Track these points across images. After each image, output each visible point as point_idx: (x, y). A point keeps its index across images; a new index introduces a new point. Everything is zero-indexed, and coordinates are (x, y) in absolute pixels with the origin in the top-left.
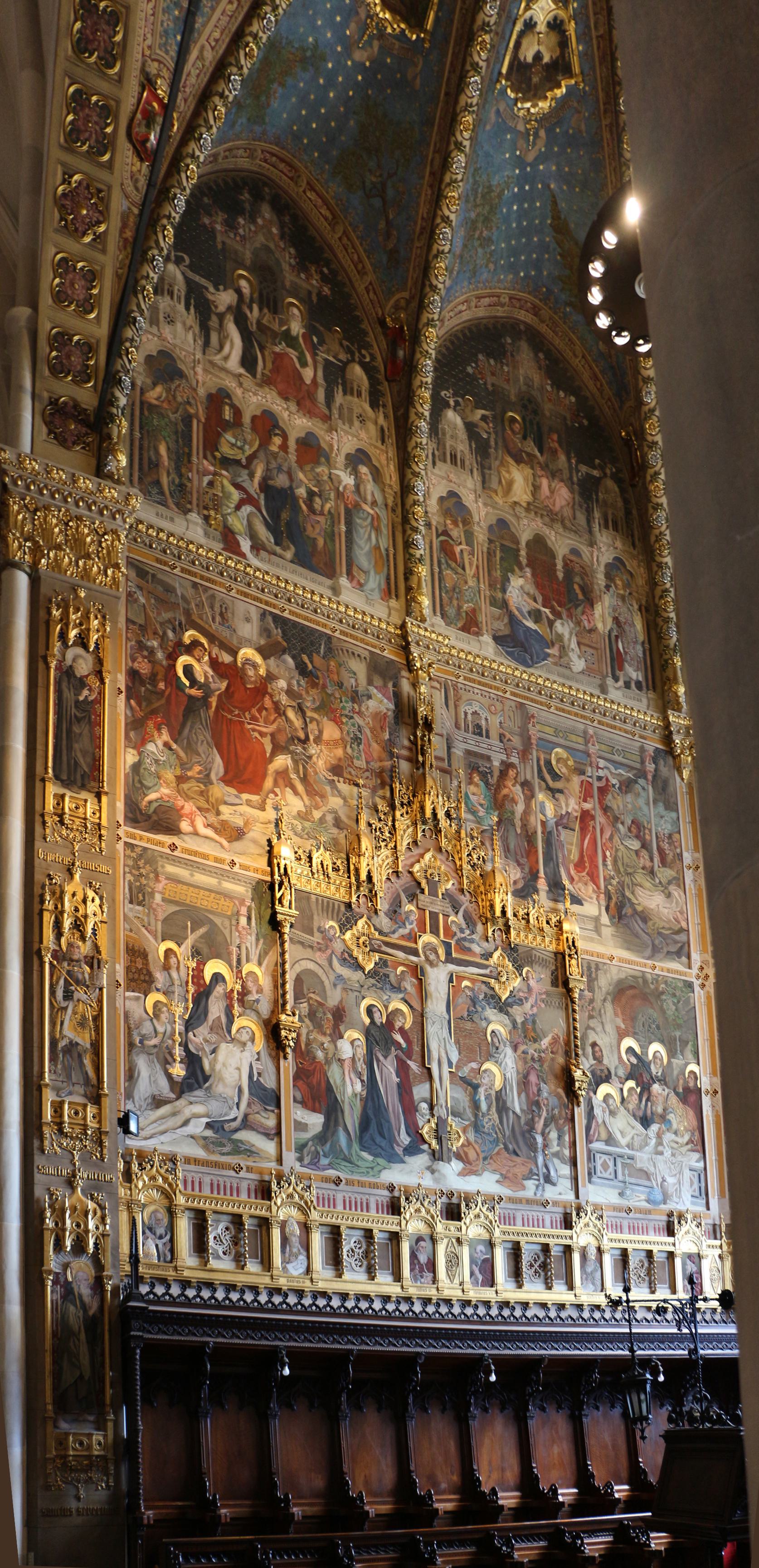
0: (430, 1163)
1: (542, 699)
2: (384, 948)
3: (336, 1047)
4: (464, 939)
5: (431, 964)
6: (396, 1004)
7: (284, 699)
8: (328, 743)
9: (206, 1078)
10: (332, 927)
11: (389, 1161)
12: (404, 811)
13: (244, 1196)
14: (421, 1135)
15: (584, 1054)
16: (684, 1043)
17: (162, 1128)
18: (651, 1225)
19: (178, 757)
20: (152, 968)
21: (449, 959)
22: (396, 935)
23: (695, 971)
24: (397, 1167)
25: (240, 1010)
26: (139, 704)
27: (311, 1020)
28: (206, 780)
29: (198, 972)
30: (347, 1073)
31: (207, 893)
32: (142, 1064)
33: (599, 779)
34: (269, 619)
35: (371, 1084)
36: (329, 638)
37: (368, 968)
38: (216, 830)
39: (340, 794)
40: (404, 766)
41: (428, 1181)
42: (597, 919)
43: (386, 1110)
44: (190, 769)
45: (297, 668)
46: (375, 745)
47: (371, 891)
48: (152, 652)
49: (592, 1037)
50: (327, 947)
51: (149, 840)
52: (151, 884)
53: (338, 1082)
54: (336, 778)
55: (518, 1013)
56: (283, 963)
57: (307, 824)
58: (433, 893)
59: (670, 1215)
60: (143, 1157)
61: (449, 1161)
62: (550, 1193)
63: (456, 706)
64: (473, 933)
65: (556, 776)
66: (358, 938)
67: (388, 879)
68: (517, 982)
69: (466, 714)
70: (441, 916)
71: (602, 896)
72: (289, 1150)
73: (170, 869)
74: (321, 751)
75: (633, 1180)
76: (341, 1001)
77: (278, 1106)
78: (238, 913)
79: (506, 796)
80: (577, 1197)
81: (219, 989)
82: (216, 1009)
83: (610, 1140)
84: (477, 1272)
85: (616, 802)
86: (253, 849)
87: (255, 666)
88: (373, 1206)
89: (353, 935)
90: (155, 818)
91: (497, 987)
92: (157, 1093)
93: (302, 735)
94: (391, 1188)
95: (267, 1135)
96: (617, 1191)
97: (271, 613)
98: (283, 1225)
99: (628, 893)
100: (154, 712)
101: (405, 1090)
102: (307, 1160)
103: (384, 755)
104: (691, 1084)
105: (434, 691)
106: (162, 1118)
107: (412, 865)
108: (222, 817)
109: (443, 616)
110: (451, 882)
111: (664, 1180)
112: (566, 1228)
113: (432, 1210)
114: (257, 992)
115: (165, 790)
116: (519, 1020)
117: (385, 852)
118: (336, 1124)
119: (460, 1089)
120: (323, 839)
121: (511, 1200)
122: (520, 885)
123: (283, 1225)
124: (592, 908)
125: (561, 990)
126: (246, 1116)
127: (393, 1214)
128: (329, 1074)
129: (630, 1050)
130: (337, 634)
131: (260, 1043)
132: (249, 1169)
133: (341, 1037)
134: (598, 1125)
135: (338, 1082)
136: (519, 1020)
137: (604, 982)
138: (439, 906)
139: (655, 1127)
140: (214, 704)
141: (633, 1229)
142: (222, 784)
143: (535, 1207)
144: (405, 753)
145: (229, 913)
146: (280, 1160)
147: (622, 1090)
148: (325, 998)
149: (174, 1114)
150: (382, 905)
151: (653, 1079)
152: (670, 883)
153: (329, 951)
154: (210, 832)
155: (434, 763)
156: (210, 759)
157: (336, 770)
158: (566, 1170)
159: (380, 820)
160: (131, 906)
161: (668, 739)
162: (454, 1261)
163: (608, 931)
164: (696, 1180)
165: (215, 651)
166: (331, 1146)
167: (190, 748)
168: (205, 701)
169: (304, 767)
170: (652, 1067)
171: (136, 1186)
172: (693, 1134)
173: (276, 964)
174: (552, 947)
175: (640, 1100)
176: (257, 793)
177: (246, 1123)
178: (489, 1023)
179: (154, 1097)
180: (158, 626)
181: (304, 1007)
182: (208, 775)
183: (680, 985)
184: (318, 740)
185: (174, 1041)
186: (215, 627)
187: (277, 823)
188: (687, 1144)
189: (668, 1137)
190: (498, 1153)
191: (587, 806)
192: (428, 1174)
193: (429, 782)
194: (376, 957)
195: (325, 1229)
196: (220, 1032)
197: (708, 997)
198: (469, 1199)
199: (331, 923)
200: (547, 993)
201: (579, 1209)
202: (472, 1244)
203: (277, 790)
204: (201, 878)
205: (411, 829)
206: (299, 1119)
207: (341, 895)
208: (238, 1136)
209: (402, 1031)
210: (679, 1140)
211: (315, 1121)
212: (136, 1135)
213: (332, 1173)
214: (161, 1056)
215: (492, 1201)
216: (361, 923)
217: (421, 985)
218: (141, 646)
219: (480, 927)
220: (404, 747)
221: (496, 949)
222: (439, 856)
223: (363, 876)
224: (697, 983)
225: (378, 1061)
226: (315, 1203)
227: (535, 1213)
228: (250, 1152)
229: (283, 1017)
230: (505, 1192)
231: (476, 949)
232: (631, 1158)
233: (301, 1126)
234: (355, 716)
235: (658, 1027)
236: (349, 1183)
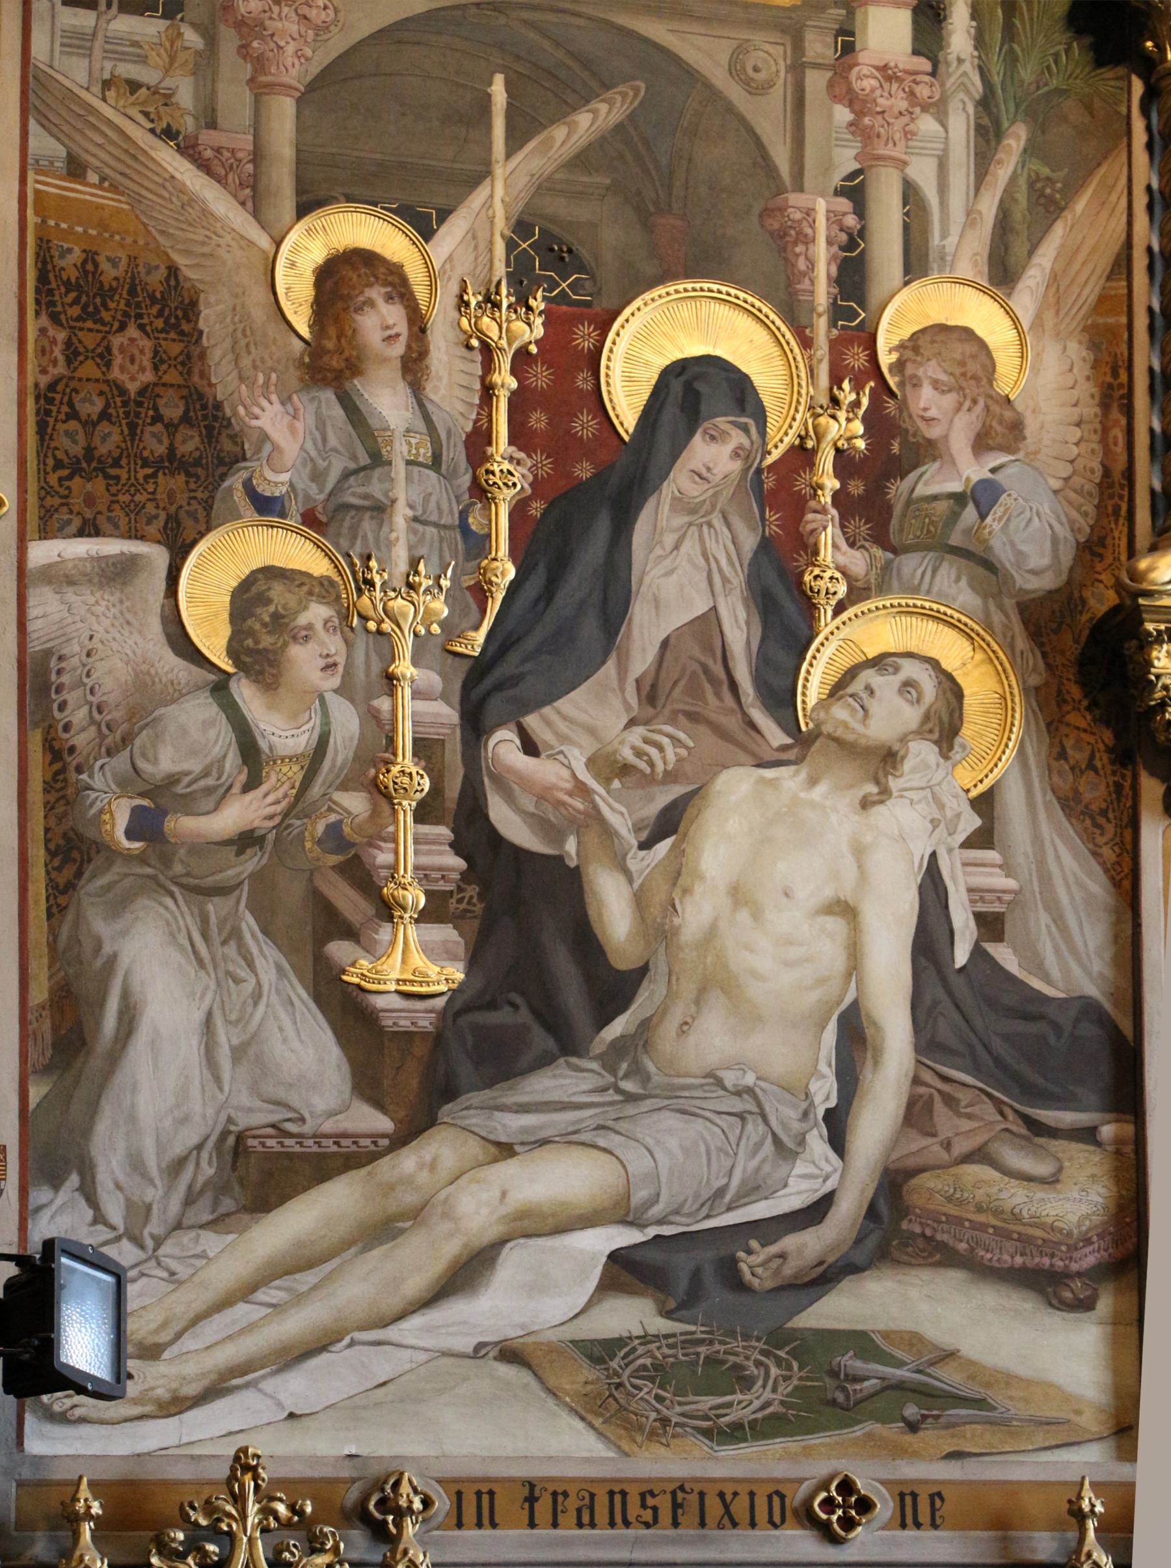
25: (857, 561)
114: (982, 444)
173: (1123, 263)
185: (383, 795)
196: (714, 704)
214: (293, 893)
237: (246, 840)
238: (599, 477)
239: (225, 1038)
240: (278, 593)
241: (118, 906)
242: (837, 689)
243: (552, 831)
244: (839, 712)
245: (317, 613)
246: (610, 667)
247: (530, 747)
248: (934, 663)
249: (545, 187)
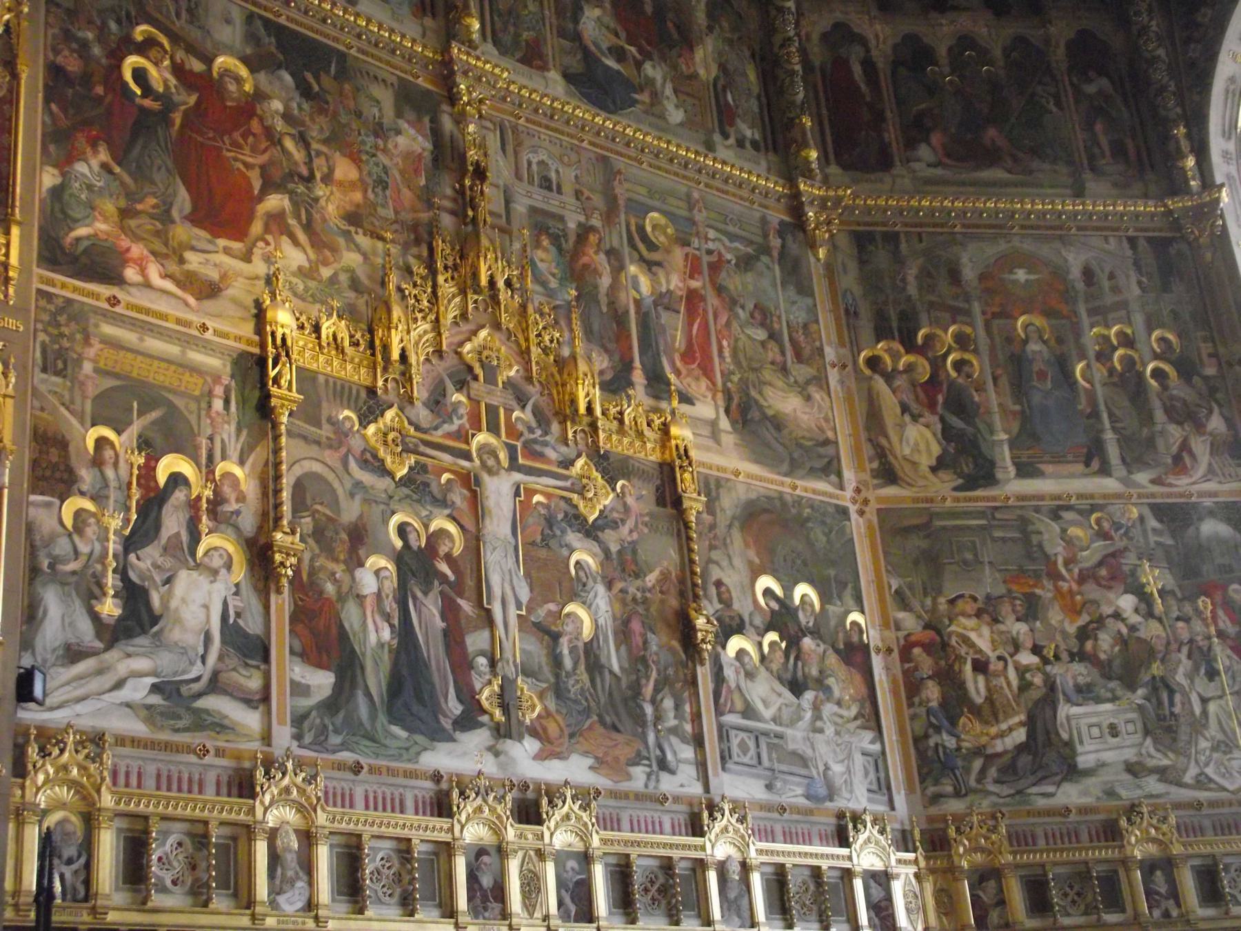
0: (491, 742)
1: (632, 153)
2: (422, 448)
3: (353, 579)
4: (535, 441)
5: (490, 472)
6: (440, 522)
7: (280, 125)
8: (340, 184)
9: (155, 620)
10: (347, 418)
11: (433, 740)
12: (449, 275)
13: (210, 794)
14: (479, 702)
15: (706, 596)
16: (844, 585)
17: (79, 692)
18: (815, 830)
19: (123, 184)
20: (74, 461)
21: (514, 466)
22: (440, 432)
23: (849, 493)
24: (443, 747)
25: (211, 524)
26: (64, 109)
27: (317, 542)
28: (165, 217)
29: (148, 470)
30: (369, 613)
31: (163, 365)
32: (53, 602)
33: (709, 252)
34: (259, 23)
35: (405, 631)
36: (342, 57)
37: (399, 475)
38: (178, 284)
39: (358, 248)
40: (447, 220)
41: (490, 766)
42: (714, 424)
43: (427, 666)
44: (141, 201)
45: (297, 87)
46: (405, 191)
47: (403, 374)
48: (84, 45)
49: (716, 573)
50: (340, 444)
51: (75, 289)
52: (78, 349)
53: (357, 626)
54: (352, 229)
55: (612, 540)
56: (277, 465)
57: (312, 284)
58: (491, 379)
59: (841, 815)
60: (48, 739)
61: (520, 739)
62: (668, 784)
63: (516, 153)
64: (546, 433)
65: (652, 247)
66: (385, 435)
67: (427, 360)
68: (608, 500)
69: (530, 163)
70: (502, 411)
71: (720, 396)
72: (281, 722)
73: (108, 329)
74: (332, 193)
75: (784, 768)
76: (361, 516)
77: (266, 659)
78: (210, 393)
79: (586, 267)
80: (707, 789)
81: (179, 495)
82: (173, 522)
83: (749, 712)
84: (568, 900)
85: (734, 282)
86: (232, 310)
87: (238, 80)
88: (409, 804)
89: (379, 429)
90: (84, 260)
91: (581, 505)
92: (73, 641)
93: (304, 171)
94: (437, 777)
95: (248, 702)
96: (762, 783)
97: (261, 17)
98: (272, 835)
99: (753, 393)
100: (86, 123)
101: (453, 638)
102: (308, 739)
103: (419, 205)
104: (855, 639)
105: (484, 131)
106: (80, 678)
107: (461, 344)
108: (187, 267)
109: (496, 43)
110: (516, 368)
111: (827, 768)
112: (694, 835)
113: (499, 809)
114: (238, 500)
115: (101, 226)
116: (614, 548)
117: (424, 326)
118: (353, 686)
119: (533, 639)
120: (336, 304)
121: (614, 795)
122: (608, 377)
123: (272, 835)
124: (706, 409)
125: (670, 510)
126: (215, 675)
127: (440, 815)
128: (343, 616)
129: (768, 592)
130: (353, 52)
131: (240, 573)
132: (220, 753)
133: (361, 565)
134: (730, 691)
135: (357, 626)
136: (614, 548)
137: (728, 503)
138: (498, 397)
139: (809, 696)
140: (178, 122)
141: (789, 837)
142: (188, 224)
143: (648, 804)
144: (448, 204)
145: (197, 393)
146: (267, 738)
147: (760, 645)
148: (338, 511)
149: (100, 672)
150: (420, 392)
151: (803, 632)
152: (808, 383)
153: (344, 450)
154: (169, 285)
155: (489, 219)
156: (170, 190)
157: (353, 218)
158: (688, 752)
159: (415, 285)
160: (43, 376)
161: (796, 207)
162: (532, 886)
163: (729, 439)
164: (872, 770)
165: (180, 55)
166: (345, 717)
167: (141, 173)
168: (164, 116)
169: (307, 210)
170: (801, 615)
171: (34, 782)
172: (862, 707)
173: (266, 464)
174: (655, 457)
175: (787, 657)
176: (236, 239)
177: (215, 685)
178: (572, 551)
179: (68, 647)
180: (95, 14)
181: (307, 522)
182: (168, 212)
183: (831, 510)
184: (328, 179)
185: (104, 564)
186: (181, 25)
187: (269, 280)
188: (856, 718)
189: (829, 709)
190: (590, 728)
191: (695, 284)
192: (490, 758)
193: (485, 242)
194: (412, 460)
195: (336, 840)
196: (179, 554)
197: (870, 527)
198: (553, 794)
199: (347, 413)
200: (650, 514)
201: (712, 808)
202: (560, 858)
203: (269, 238)
204: (155, 345)
205: (458, 299)
206: (297, 678)
207: (362, 377)
208: (201, 703)
209: (448, 558)
210: (845, 713)
211: (322, 681)
212: (40, 703)
213: (347, 756)
215: (586, 796)
216: (390, 414)
217: (475, 500)
218: (68, 36)
219: (555, 427)
220: (445, 197)
221: (579, 456)
222: (497, 335)
223: (395, 355)
224: (853, 509)
225: (415, 598)
226: (322, 801)
227: (646, 813)
228: (221, 726)
229: (279, 536)
230: (600, 781)
231: (552, 454)
232: (779, 736)
233: (299, 689)
234: (379, 154)
235: (805, 564)
236: (372, 770)
237: (74, 573)
238: (155, 498)
239: (67, 620)
240: (84, 515)
241: (44, 585)
242: (206, 554)
243: (143, 580)
244: (206, 559)
245: (92, 520)
246: (156, 542)
247: (138, 559)
248: (226, 550)
249: (145, 428)
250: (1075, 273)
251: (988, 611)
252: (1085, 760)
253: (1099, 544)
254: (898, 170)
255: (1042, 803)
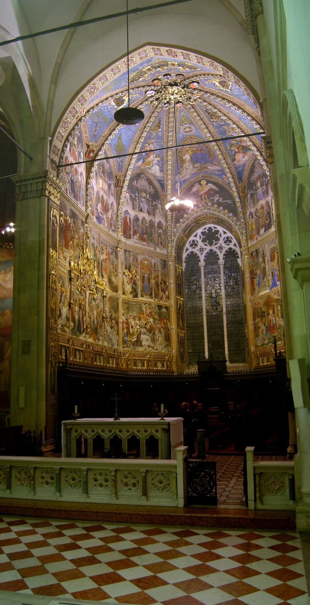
250: (153, 264)
251: (134, 318)
252: (143, 344)
253: (150, 310)
254: (132, 239)
255: (137, 350)
